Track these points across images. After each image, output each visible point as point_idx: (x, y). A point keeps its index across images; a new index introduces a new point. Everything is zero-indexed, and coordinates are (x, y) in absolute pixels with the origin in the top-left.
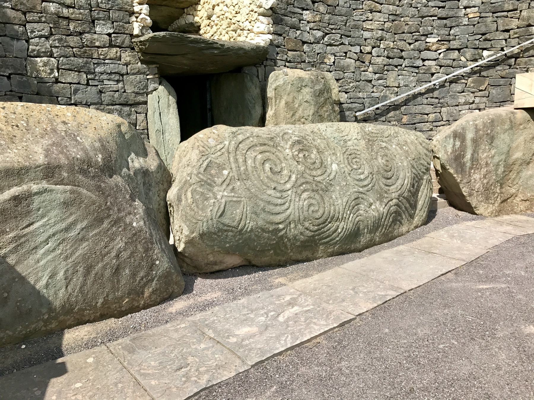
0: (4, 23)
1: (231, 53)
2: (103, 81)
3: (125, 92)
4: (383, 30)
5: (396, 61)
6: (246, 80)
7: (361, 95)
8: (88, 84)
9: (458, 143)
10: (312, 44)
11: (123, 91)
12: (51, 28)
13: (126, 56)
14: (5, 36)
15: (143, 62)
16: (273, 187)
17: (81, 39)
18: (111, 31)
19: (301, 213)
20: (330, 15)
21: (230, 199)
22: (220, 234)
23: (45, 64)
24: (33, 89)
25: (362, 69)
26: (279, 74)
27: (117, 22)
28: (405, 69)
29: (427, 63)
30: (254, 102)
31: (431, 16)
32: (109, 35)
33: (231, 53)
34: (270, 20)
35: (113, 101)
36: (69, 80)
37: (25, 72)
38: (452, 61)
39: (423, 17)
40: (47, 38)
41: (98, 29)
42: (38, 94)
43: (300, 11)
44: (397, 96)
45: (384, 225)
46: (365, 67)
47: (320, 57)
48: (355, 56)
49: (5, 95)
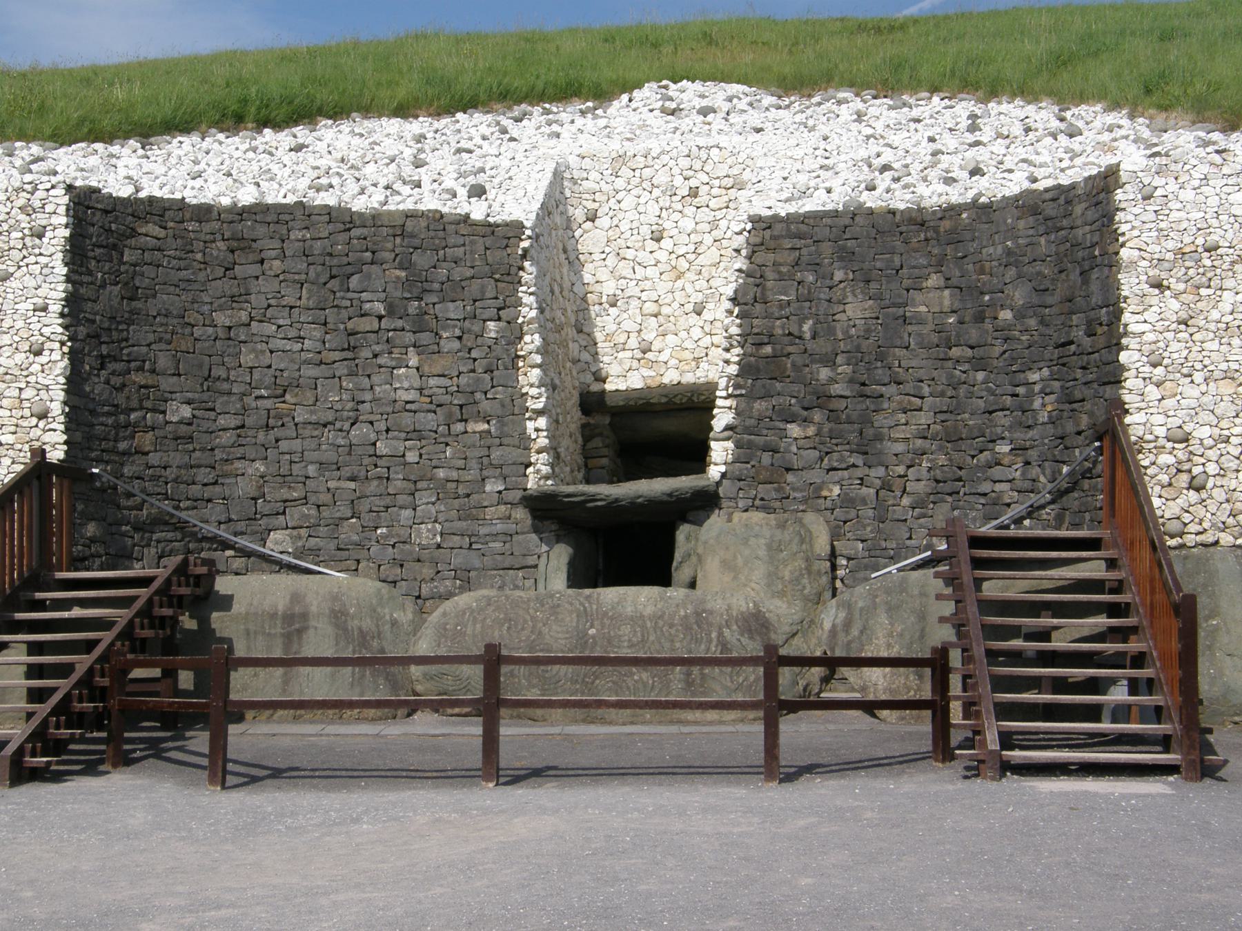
4: (925, 438)
5: (947, 487)
9: (842, 615)
15: (534, 517)
18: (501, 488)
20: (832, 425)
23: (428, 530)
25: (890, 503)
29: (998, 487)
31: (1002, 410)
32: (500, 492)
34: (730, 445)
36: (451, 545)
38: (1030, 483)
39: (991, 413)
41: (488, 488)
42: (419, 561)
43: (781, 425)
48: (878, 482)
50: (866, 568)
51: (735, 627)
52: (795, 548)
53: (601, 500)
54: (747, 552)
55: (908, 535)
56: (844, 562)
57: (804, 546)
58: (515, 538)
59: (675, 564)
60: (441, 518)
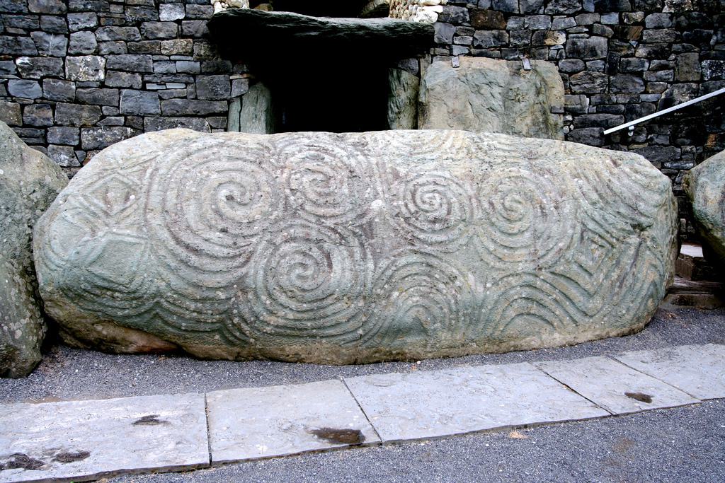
0: (40, 14)
1: (342, 34)
2: (165, 84)
3: (196, 98)
6: (390, 78)
7: (621, 100)
8: (143, 89)
10: (523, 16)
11: (192, 97)
12: (99, 18)
13: (201, 49)
14: (40, 30)
16: (220, 227)
17: (139, 29)
18: (181, 16)
19: (270, 278)
21: (120, 238)
22: (98, 292)
24: (70, 96)
26: (444, 66)
27: (190, 3)
28: (716, 47)
30: (397, 110)
32: (178, 22)
33: (342, 34)
35: (178, 112)
36: (118, 84)
37: (62, 74)
40: (93, 30)
41: (164, 15)
42: (77, 101)
44: (696, 97)
45: (488, 321)
46: (629, 48)
47: (538, 36)
49: (35, 103)
50: (594, 124)
51: (595, 197)
52: (531, 96)
53: (315, 29)
54: (477, 101)
55: (642, 89)
56: (569, 118)
57: (541, 98)
58: (200, 79)
59: (391, 115)
60: (104, 50)
